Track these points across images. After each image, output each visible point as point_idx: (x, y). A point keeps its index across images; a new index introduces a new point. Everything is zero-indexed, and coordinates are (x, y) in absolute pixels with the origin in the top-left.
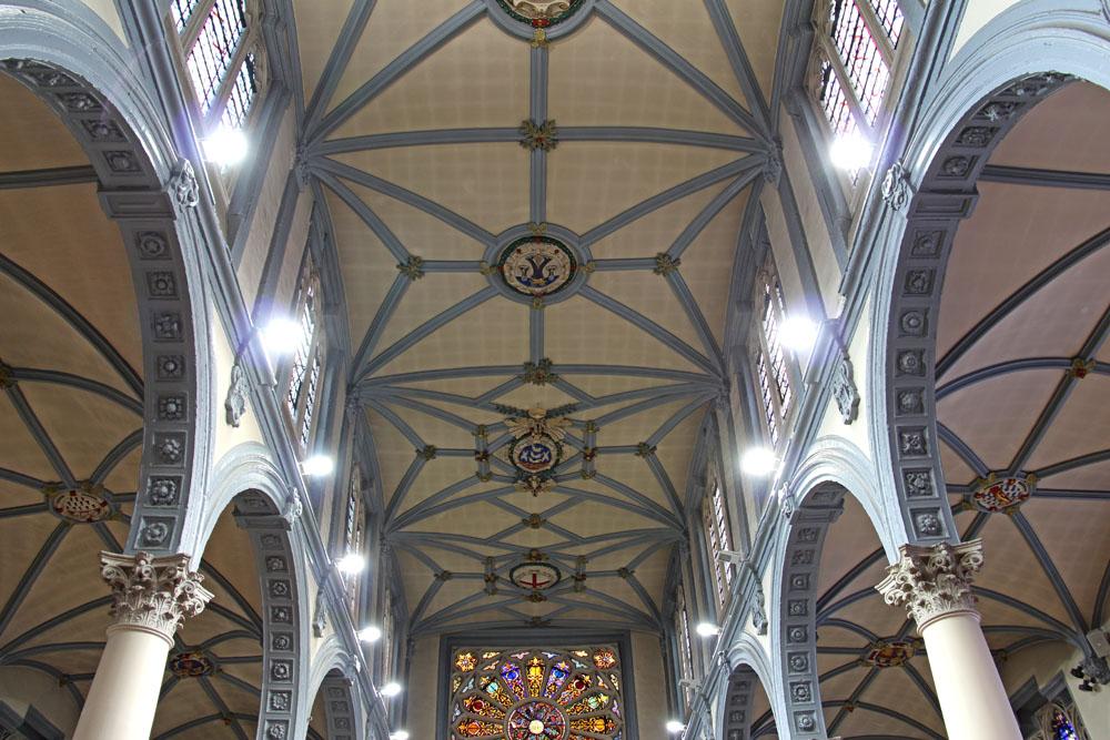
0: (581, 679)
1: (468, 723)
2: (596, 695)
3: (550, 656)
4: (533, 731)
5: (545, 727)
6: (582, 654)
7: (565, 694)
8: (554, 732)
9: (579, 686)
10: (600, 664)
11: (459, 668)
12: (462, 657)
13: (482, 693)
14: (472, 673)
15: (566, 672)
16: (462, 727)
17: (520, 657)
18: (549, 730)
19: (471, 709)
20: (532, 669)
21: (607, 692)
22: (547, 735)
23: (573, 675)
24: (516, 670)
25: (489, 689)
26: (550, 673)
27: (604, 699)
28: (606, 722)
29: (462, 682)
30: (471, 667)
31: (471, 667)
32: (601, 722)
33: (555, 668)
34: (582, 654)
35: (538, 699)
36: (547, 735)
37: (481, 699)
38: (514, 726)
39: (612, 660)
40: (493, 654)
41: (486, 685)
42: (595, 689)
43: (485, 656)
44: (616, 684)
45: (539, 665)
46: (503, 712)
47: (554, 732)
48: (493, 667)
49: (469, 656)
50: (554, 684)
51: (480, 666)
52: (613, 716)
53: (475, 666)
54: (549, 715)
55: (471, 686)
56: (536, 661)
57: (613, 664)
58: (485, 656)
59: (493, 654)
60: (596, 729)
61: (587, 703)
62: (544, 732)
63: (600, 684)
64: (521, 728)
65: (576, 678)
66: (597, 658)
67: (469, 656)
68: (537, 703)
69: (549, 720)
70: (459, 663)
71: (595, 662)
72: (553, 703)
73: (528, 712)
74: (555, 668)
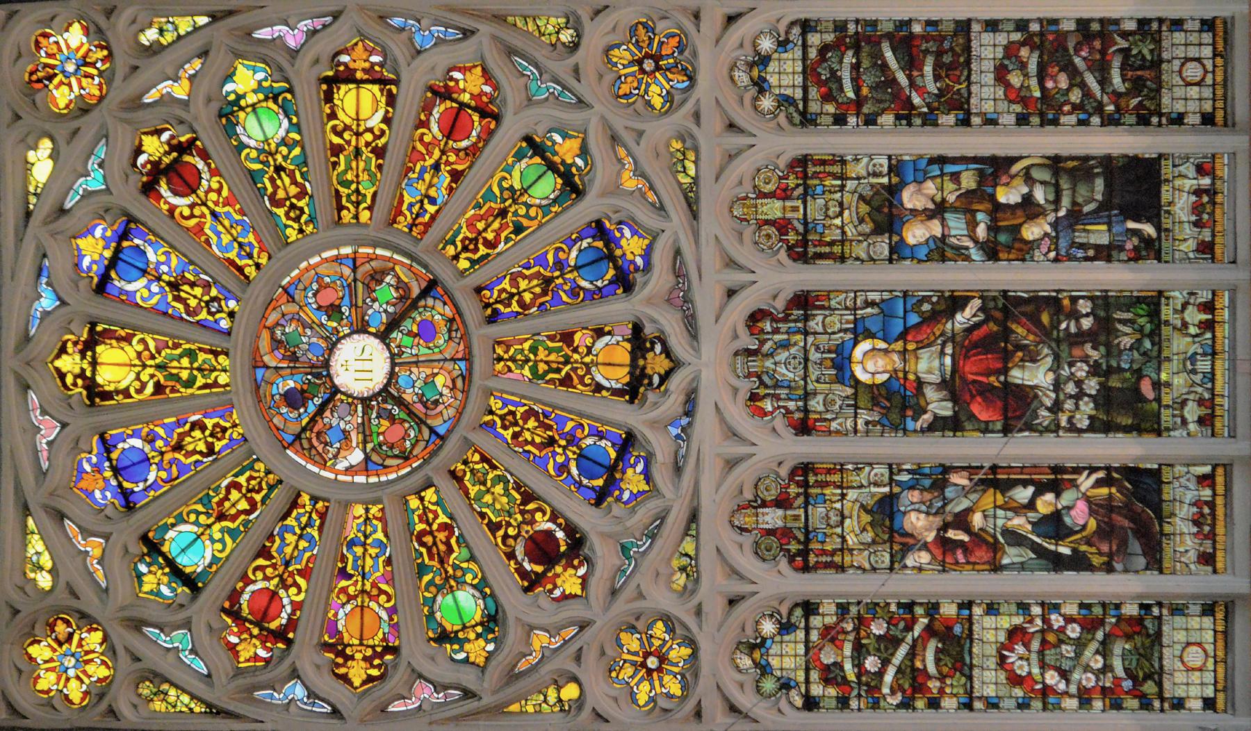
0: (157, 171)
1: (339, 650)
2: (229, 112)
3: (47, 302)
4: (378, 378)
5: (362, 328)
6: (41, 166)
7: (221, 242)
8: (386, 293)
9: (187, 183)
10: (92, 88)
11: (99, 692)
12: (47, 681)
13: (213, 594)
14: (124, 637)
15: (124, 235)
16: (357, 672)
17: (49, 430)
18: (377, 319)
19: (280, 635)
20: (106, 377)
21: (219, 58)
22: (394, 324)
23: (139, 207)
24: (107, 446)
25: (192, 561)
26: (129, 301)
27: (246, 80)
28: (348, 77)
29: (157, 677)
30: (94, 639)
31: (94, 639)
32: (346, 97)
33: (105, 279)
34: (41, 166)
35: (242, 355)
36: (394, 324)
37: (235, 596)
38: (357, 457)
39: (75, 36)
40: (36, 544)
41: (177, 572)
42: (204, 119)
43: (45, 581)
44: (185, 25)
45: (89, 346)
46: (294, 504)
47: (386, 293)
48: (94, 546)
49: (40, 652)
50: (174, 286)
51: (90, 602)
52: (324, 46)
53: (87, 620)
54: (310, 314)
55: (180, 639)
56: (70, 363)
57: (94, 31)
58: (45, 581)
59: (36, 544)
60: (375, 122)
61: (266, 153)
62: (383, 336)
63: (180, 91)
64: (365, 431)
65: (149, 189)
66: (62, 97)
67: (40, 652)
68: (257, 363)
69: (333, 310)
70: (75, 691)
71: (83, 108)
72: (258, 293)
73: (294, 399)
74: (105, 279)
